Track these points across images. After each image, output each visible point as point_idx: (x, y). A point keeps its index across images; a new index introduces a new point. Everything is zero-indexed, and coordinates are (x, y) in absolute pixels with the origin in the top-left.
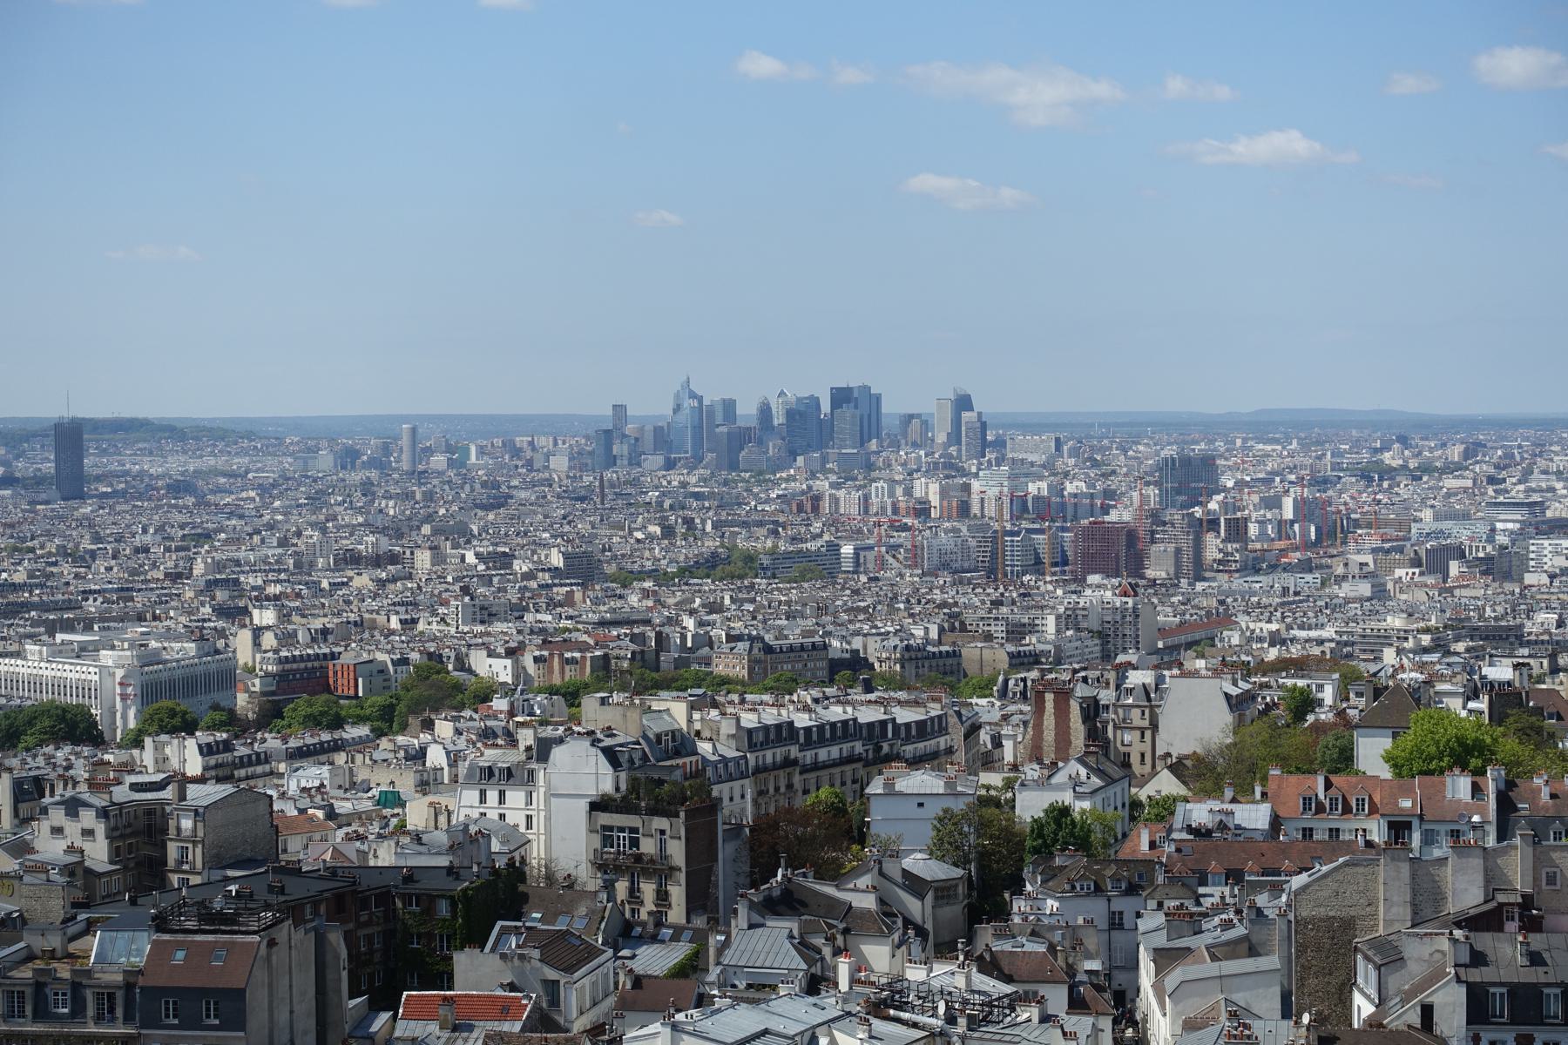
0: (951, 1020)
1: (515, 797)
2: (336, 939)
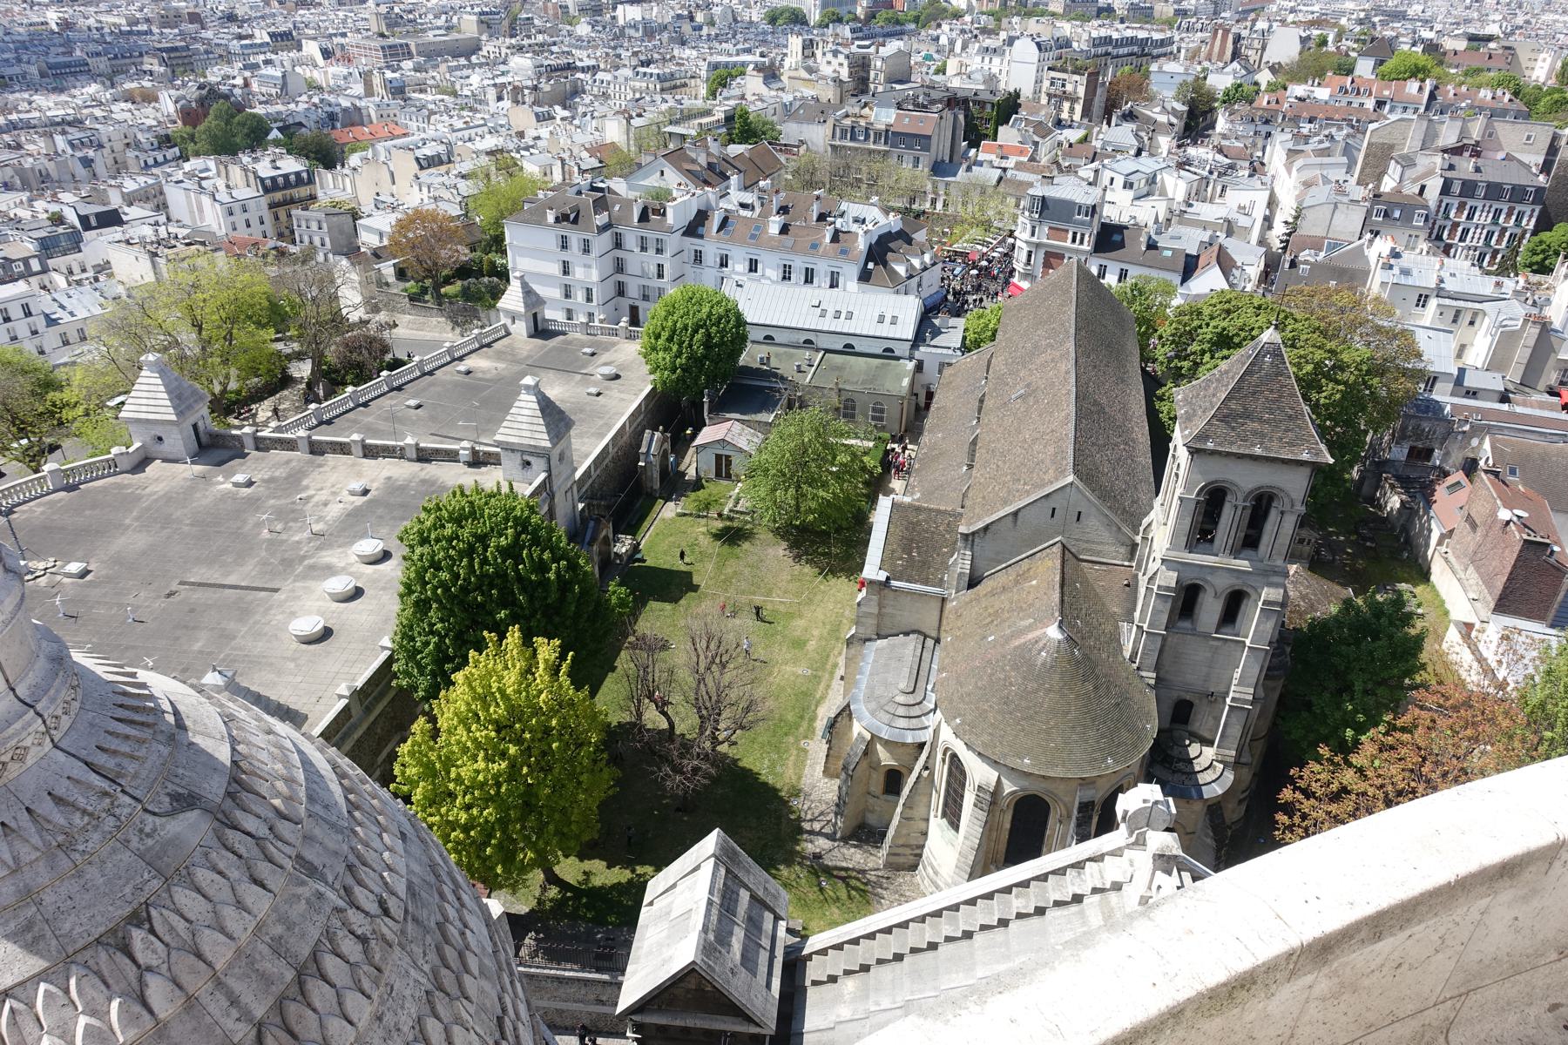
0: (1211, 172)
1: (996, 60)
2: (961, 117)
